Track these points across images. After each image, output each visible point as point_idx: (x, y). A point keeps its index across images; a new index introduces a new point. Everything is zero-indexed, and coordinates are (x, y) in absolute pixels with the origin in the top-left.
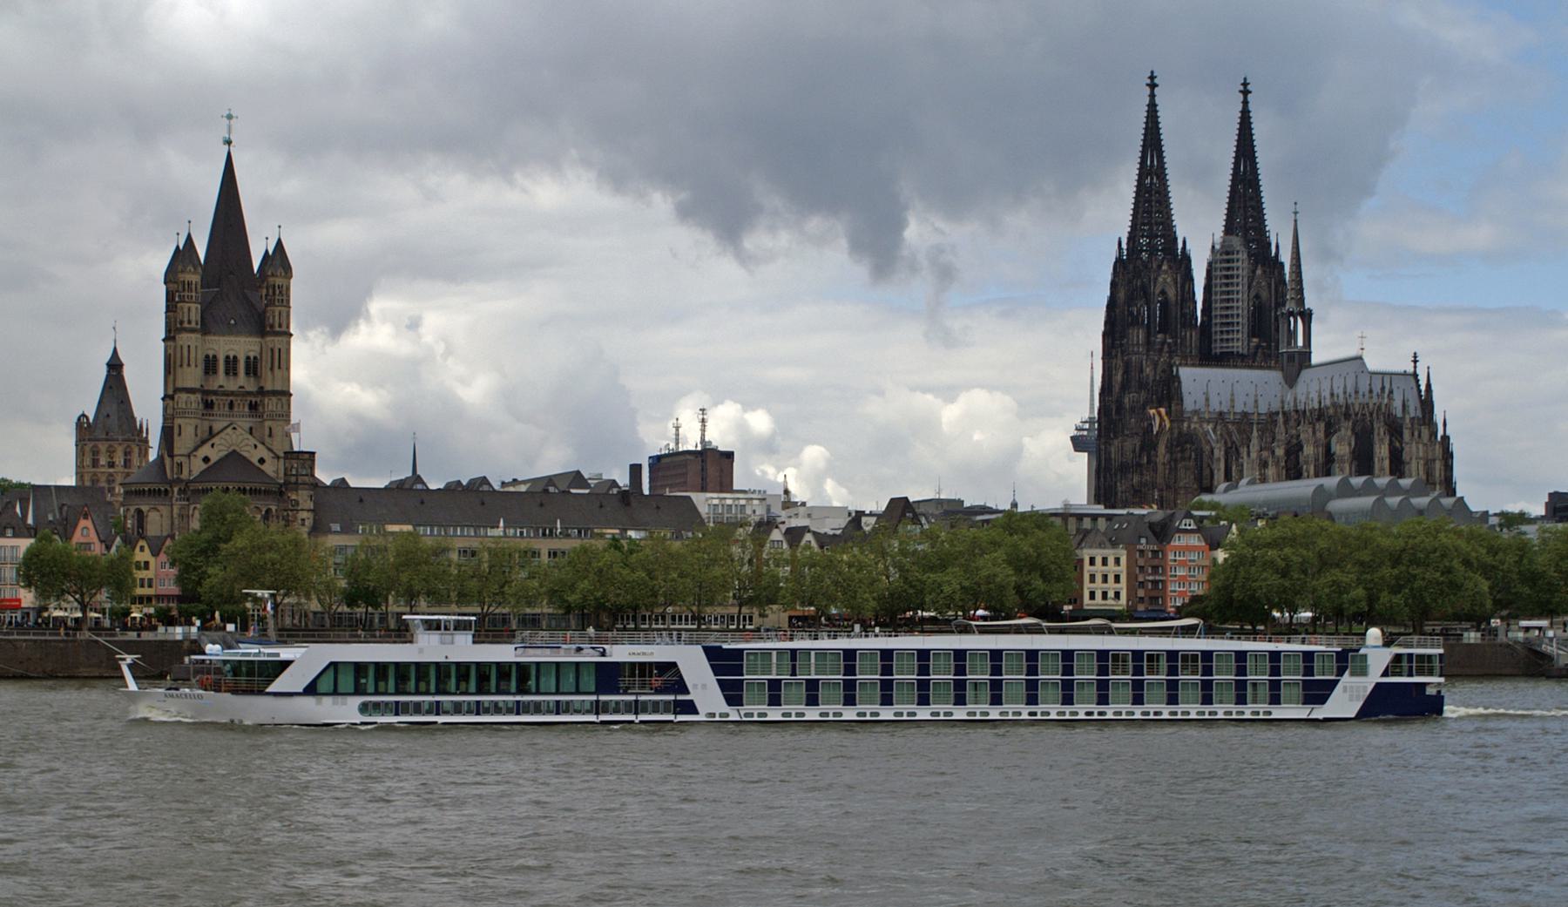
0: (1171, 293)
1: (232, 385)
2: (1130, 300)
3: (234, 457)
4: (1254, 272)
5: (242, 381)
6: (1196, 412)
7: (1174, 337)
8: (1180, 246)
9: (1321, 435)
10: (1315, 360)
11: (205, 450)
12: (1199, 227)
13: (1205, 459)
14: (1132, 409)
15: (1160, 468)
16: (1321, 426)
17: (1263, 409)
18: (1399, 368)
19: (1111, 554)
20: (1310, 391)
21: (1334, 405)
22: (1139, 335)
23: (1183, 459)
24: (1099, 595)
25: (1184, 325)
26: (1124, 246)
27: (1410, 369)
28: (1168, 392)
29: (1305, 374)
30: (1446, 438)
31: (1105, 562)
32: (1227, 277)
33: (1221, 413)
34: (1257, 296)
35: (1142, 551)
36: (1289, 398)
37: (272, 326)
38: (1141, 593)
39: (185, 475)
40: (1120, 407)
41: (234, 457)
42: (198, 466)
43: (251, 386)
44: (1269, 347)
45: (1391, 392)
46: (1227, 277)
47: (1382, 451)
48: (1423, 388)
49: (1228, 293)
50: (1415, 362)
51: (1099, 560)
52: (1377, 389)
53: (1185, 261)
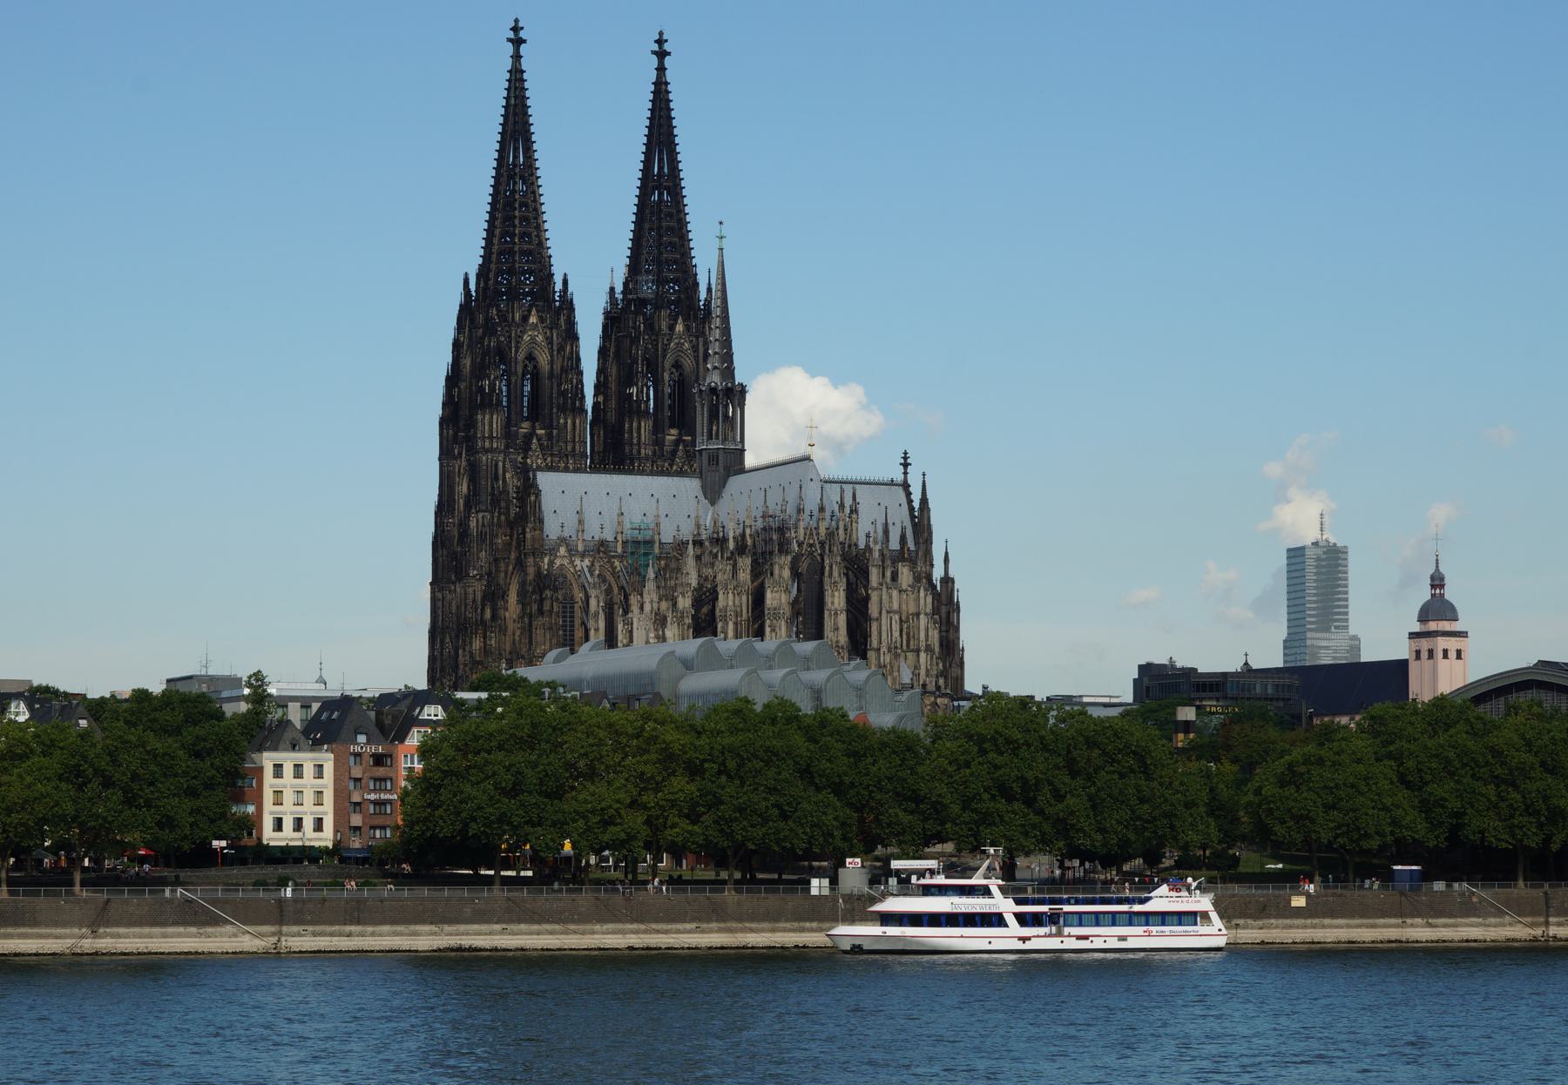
0: (543, 359)
2: (480, 371)
6: (563, 540)
7: (549, 427)
8: (559, 286)
9: (745, 576)
10: (750, 460)
12: (589, 256)
13: (578, 613)
14: (482, 537)
15: (511, 626)
16: (745, 563)
17: (667, 537)
18: (885, 476)
19: (308, 759)
20: (740, 506)
24: (288, 824)
25: (563, 409)
26: (472, 286)
27: (899, 478)
28: (524, 508)
29: (735, 483)
30: (947, 581)
31: (298, 770)
33: (602, 543)
35: (357, 755)
36: (708, 521)
38: (356, 820)
40: (464, 533)
45: (854, 511)
48: (916, 505)
50: (906, 465)
51: (288, 770)
52: (832, 502)
53: (561, 312)
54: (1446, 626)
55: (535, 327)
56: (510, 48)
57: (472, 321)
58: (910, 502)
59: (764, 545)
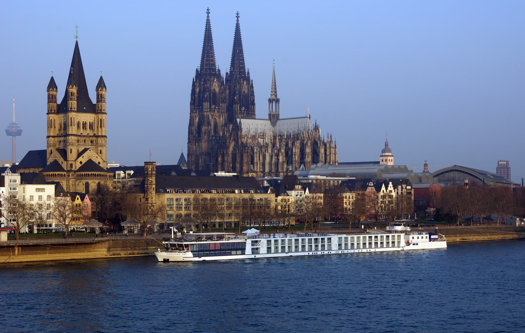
1: (85, 134)
3: (90, 161)
5: (88, 131)
6: (246, 135)
10: (281, 117)
11: (80, 159)
14: (205, 132)
20: (286, 127)
23: (245, 152)
29: (278, 121)
33: (253, 136)
37: (101, 110)
39: (73, 169)
41: (90, 161)
42: (78, 165)
43: (91, 134)
44: (248, 110)
57: (200, 80)
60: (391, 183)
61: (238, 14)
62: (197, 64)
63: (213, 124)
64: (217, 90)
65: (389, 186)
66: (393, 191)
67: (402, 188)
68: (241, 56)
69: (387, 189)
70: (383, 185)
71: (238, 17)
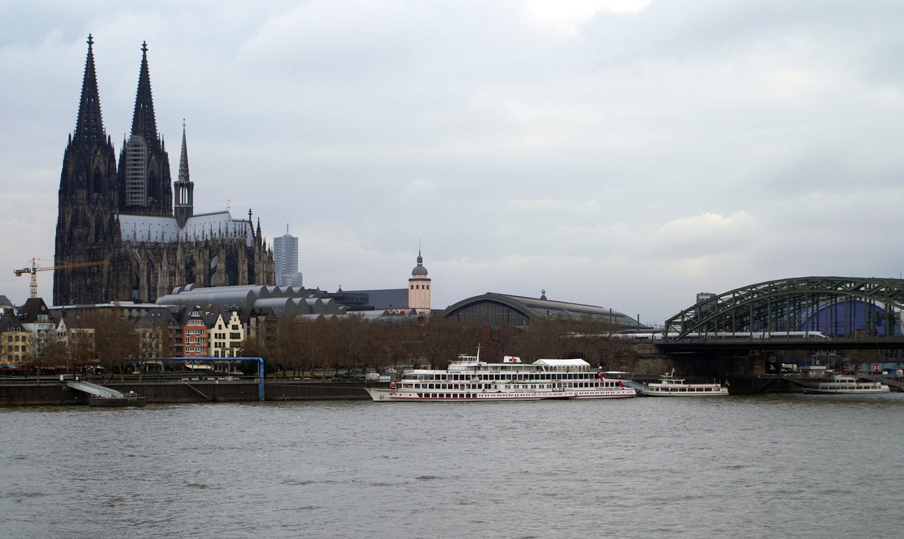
4: (150, 158)
6: (129, 242)
9: (207, 257)
10: (195, 213)
13: (134, 270)
17: (167, 240)
20: (195, 229)
21: (212, 239)
22: (82, 193)
23: (123, 270)
29: (191, 221)
32: (135, 160)
33: (143, 243)
34: (152, 172)
40: (71, 238)
44: (159, 203)
46: (135, 160)
47: (243, 267)
48: (255, 230)
49: (136, 170)
50: (250, 214)
54: (423, 277)
55: (99, 156)
56: (88, 45)
58: (252, 229)
59: (210, 247)
60: (235, 313)
61: (144, 45)
62: (70, 126)
63: (93, 224)
64: (103, 169)
65: (232, 318)
66: (240, 326)
67: (257, 321)
68: (148, 114)
69: (226, 324)
70: (220, 317)
71: (145, 50)
